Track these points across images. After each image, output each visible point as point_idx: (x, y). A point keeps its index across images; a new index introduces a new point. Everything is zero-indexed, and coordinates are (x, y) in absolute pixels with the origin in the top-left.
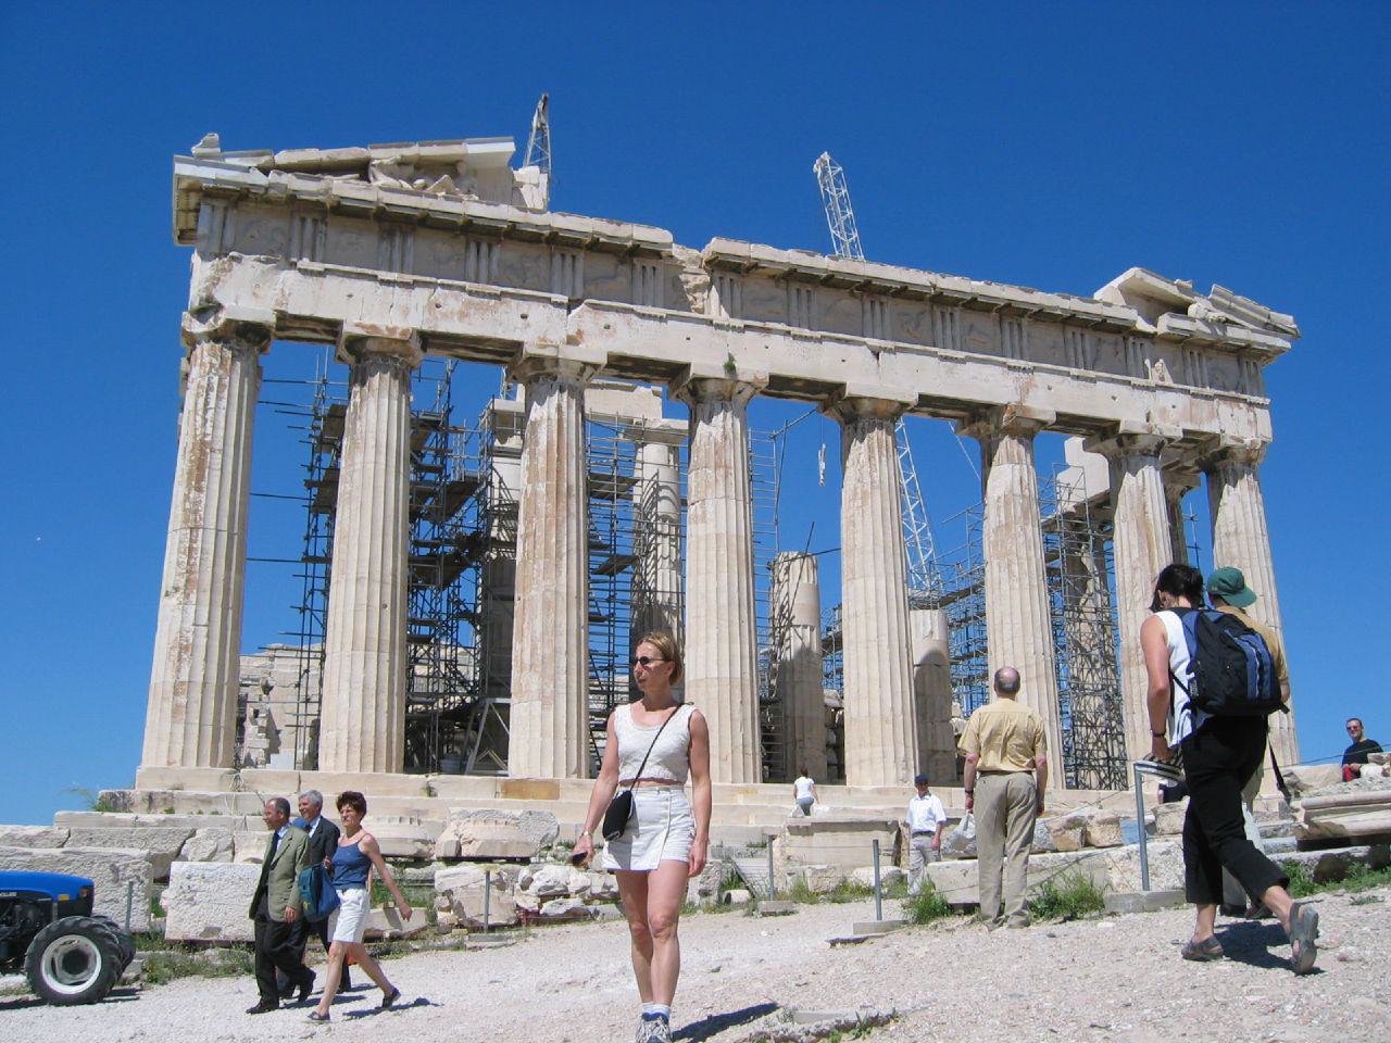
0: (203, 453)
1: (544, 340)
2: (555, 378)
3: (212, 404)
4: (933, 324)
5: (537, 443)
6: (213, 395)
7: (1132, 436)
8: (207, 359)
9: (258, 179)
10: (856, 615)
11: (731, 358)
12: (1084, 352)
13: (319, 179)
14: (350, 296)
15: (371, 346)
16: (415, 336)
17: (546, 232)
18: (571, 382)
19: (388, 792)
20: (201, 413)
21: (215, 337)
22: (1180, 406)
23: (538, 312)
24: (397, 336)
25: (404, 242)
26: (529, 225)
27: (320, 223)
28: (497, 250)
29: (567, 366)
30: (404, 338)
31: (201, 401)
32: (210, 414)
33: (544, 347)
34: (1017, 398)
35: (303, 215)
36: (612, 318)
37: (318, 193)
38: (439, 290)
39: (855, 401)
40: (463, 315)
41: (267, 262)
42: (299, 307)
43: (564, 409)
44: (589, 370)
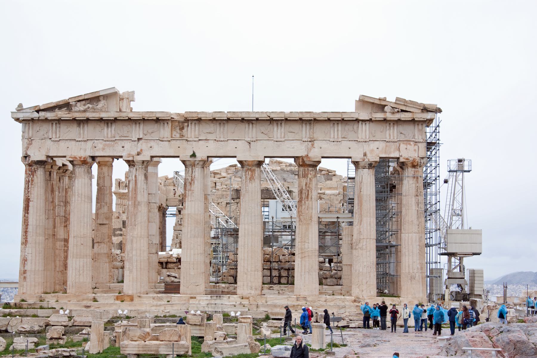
0: (28, 202)
2: (134, 166)
4: (274, 129)
6: (30, 183)
7: (357, 162)
12: (338, 130)
13: (54, 112)
15: (75, 163)
17: (127, 118)
22: (380, 149)
23: (127, 145)
25: (83, 127)
33: (129, 157)
34: (306, 154)
36: (152, 143)
44: (145, 163)
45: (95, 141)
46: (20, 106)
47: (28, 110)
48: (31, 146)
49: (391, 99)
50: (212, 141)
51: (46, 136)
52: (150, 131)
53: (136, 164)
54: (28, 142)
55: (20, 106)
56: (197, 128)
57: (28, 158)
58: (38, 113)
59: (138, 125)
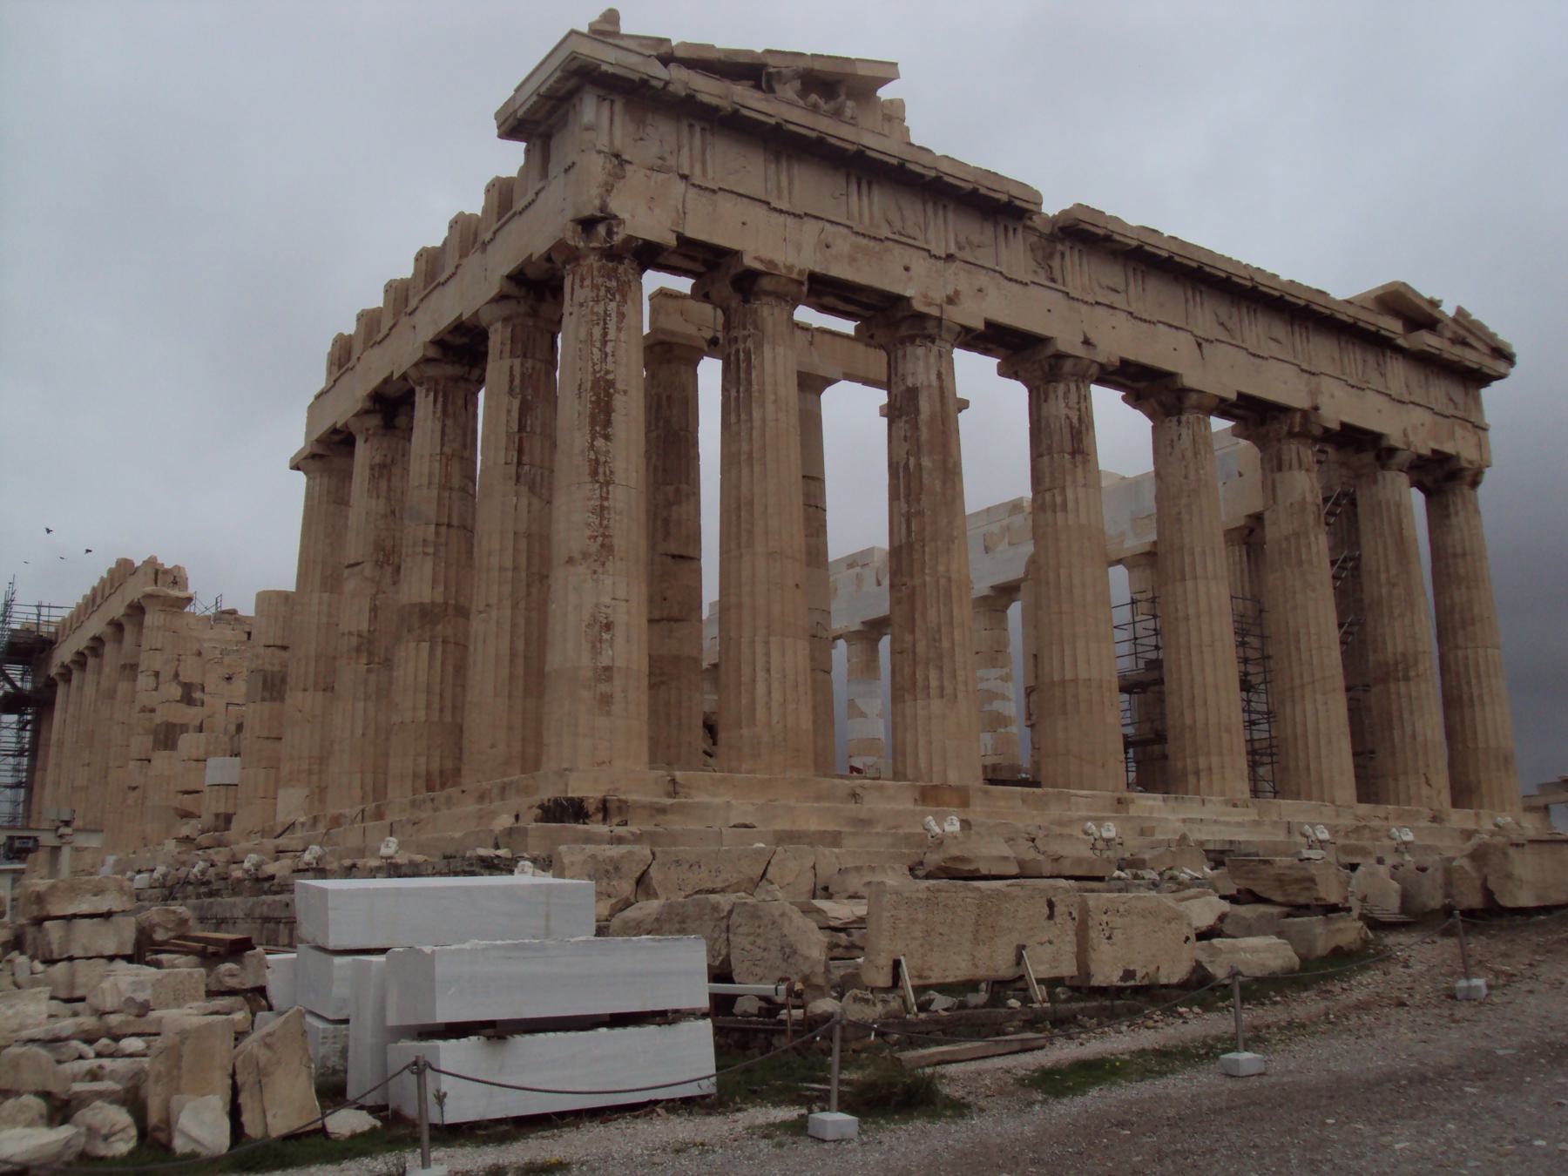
0: (610, 396)
2: (933, 342)
3: (612, 334)
4: (1241, 321)
5: (917, 411)
7: (1392, 451)
8: (600, 281)
9: (659, 71)
10: (1187, 618)
17: (933, 174)
19: (818, 798)
20: (598, 344)
21: (611, 254)
23: (920, 265)
24: (795, 276)
31: (597, 332)
32: (609, 349)
33: (929, 304)
36: (983, 279)
39: (1187, 390)
40: (852, 260)
42: (697, 230)
45: (828, 225)
46: (612, 17)
48: (619, 185)
49: (1449, 309)
50: (1123, 316)
51: (671, 161)
54: (609, 166)
55: (612, 17)
57: (601, 229)
59: (941, 212)
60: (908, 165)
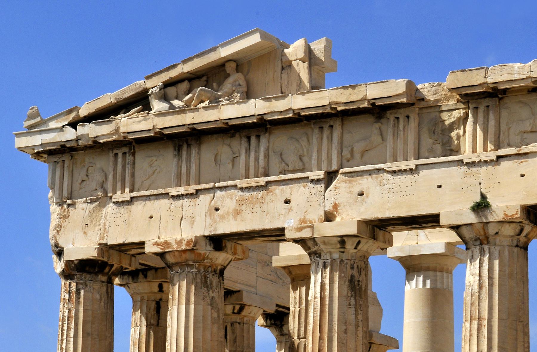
1: (303, 221)
2: (320, 256)
11: (483, 197)
14: (151, 217)
16: (203, 243)
18: (336, 256)
24: (184, 247)
26: (272, 113)
27: (127, 155)
28: (264, 141)
29: (324, 243)
30: (188, 248)
33: (300, 229)
35: (116, 151)
36: (365, 182)
37: (111, 134)
38: (219, 193)
41: (92, 202)
42: (115, 238)
43: (327, 287)
47: (53, 125)
52: (358, 147)
53: (322, 247)
56: (492, 122)
58: (75, 128)
60: (265, 117)
